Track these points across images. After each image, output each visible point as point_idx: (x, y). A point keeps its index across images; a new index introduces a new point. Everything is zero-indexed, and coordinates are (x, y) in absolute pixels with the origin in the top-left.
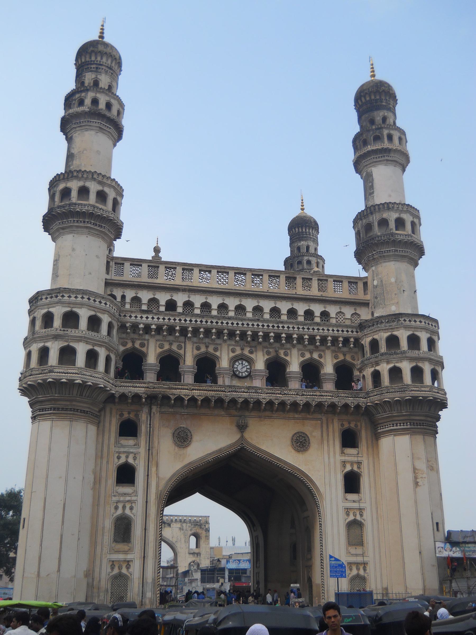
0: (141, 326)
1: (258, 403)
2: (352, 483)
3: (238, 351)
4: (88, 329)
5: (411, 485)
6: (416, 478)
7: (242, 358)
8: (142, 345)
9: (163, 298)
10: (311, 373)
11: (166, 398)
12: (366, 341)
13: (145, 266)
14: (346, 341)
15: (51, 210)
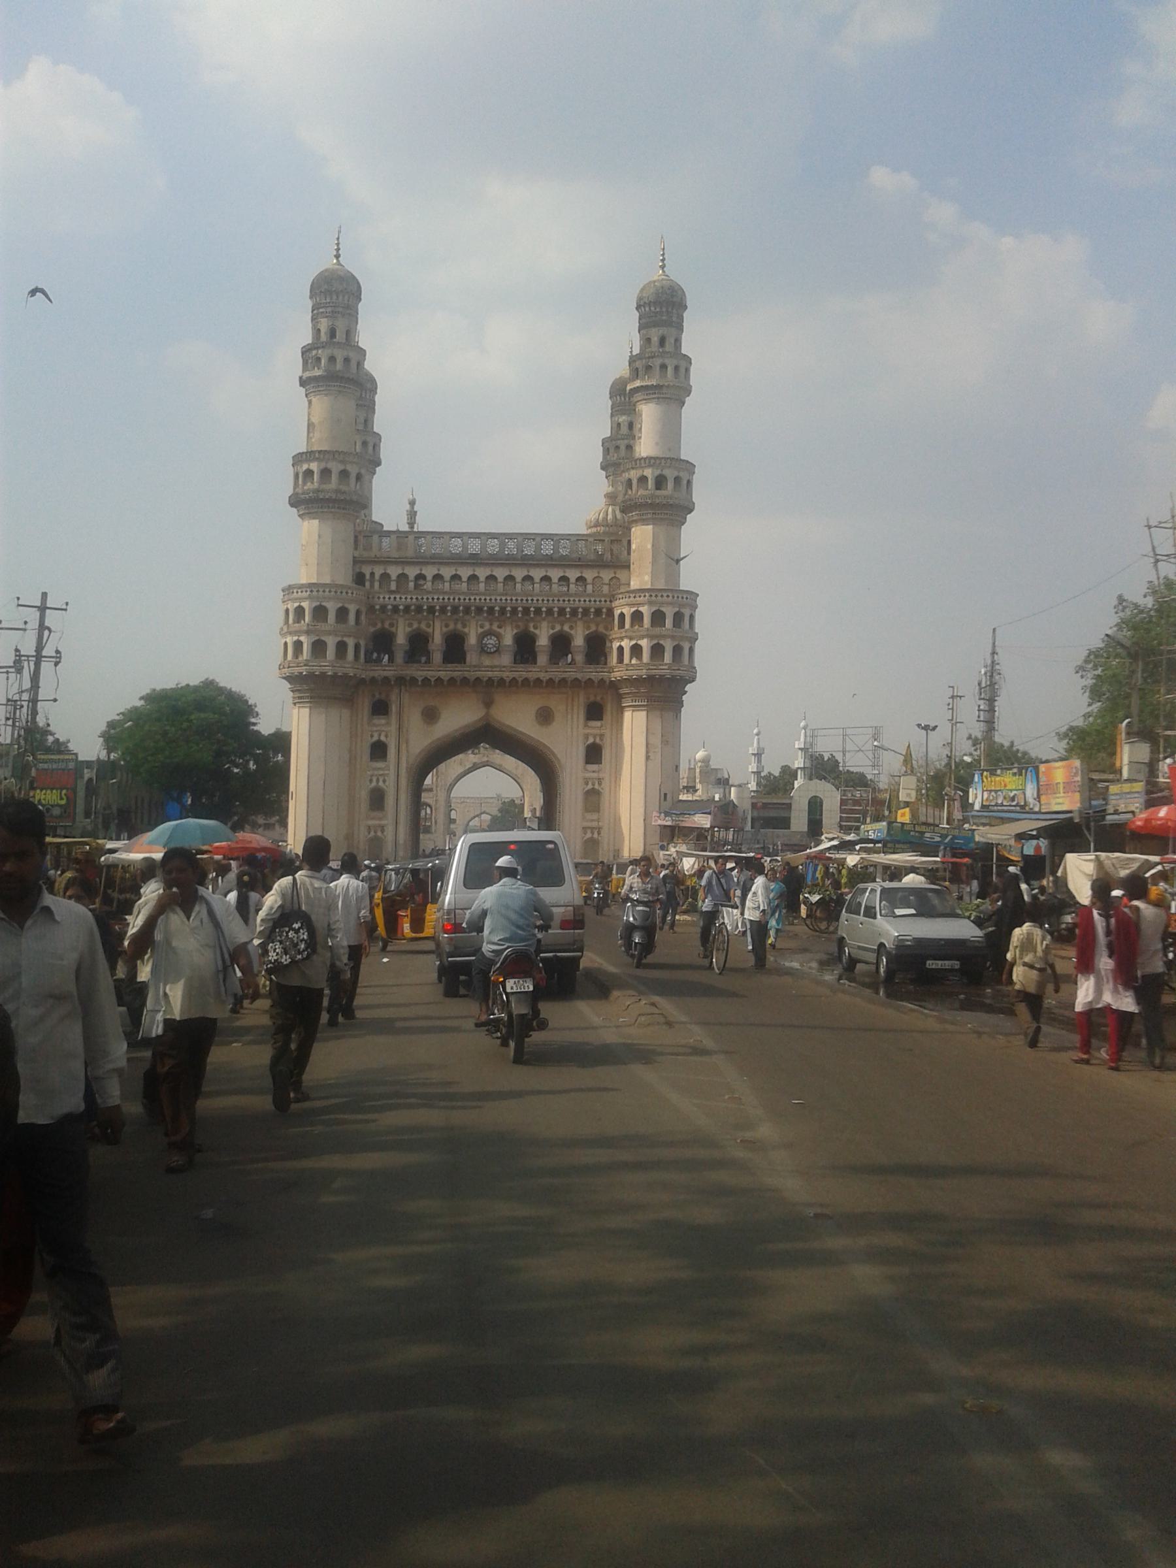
0: (390, 607)
1: (502, 682)
2: (594, 754)
3: (487, 626)
4: (337, 622)
5: (643, 759)
6: (647, 752)
7: (490, 633)
8: (392, 625)
9: (412, 572)
10: (561, 644)
11: (413, 680)
12: (617, 612)
13: (393, 537)
14: (598, 612)
15: (295, 494)
